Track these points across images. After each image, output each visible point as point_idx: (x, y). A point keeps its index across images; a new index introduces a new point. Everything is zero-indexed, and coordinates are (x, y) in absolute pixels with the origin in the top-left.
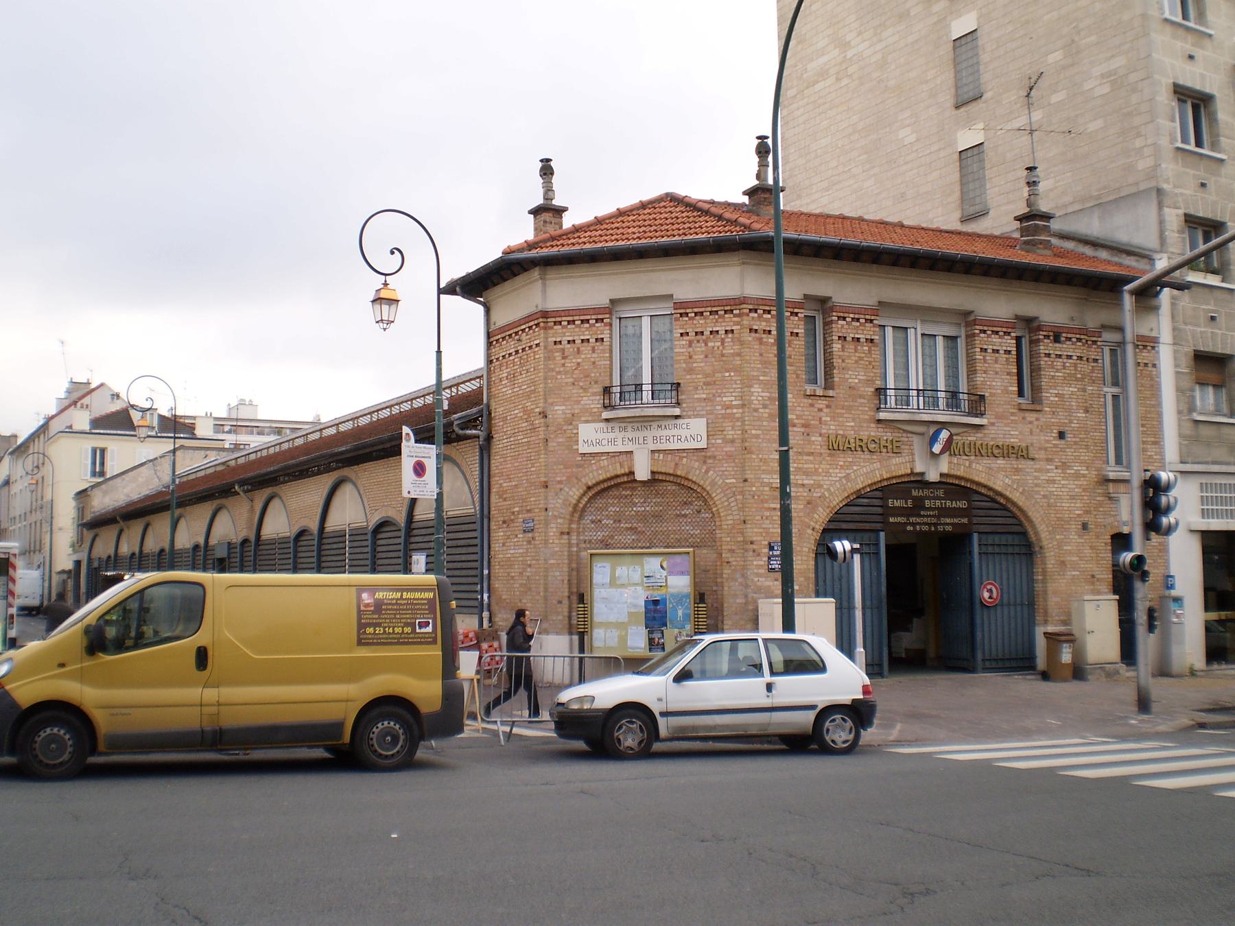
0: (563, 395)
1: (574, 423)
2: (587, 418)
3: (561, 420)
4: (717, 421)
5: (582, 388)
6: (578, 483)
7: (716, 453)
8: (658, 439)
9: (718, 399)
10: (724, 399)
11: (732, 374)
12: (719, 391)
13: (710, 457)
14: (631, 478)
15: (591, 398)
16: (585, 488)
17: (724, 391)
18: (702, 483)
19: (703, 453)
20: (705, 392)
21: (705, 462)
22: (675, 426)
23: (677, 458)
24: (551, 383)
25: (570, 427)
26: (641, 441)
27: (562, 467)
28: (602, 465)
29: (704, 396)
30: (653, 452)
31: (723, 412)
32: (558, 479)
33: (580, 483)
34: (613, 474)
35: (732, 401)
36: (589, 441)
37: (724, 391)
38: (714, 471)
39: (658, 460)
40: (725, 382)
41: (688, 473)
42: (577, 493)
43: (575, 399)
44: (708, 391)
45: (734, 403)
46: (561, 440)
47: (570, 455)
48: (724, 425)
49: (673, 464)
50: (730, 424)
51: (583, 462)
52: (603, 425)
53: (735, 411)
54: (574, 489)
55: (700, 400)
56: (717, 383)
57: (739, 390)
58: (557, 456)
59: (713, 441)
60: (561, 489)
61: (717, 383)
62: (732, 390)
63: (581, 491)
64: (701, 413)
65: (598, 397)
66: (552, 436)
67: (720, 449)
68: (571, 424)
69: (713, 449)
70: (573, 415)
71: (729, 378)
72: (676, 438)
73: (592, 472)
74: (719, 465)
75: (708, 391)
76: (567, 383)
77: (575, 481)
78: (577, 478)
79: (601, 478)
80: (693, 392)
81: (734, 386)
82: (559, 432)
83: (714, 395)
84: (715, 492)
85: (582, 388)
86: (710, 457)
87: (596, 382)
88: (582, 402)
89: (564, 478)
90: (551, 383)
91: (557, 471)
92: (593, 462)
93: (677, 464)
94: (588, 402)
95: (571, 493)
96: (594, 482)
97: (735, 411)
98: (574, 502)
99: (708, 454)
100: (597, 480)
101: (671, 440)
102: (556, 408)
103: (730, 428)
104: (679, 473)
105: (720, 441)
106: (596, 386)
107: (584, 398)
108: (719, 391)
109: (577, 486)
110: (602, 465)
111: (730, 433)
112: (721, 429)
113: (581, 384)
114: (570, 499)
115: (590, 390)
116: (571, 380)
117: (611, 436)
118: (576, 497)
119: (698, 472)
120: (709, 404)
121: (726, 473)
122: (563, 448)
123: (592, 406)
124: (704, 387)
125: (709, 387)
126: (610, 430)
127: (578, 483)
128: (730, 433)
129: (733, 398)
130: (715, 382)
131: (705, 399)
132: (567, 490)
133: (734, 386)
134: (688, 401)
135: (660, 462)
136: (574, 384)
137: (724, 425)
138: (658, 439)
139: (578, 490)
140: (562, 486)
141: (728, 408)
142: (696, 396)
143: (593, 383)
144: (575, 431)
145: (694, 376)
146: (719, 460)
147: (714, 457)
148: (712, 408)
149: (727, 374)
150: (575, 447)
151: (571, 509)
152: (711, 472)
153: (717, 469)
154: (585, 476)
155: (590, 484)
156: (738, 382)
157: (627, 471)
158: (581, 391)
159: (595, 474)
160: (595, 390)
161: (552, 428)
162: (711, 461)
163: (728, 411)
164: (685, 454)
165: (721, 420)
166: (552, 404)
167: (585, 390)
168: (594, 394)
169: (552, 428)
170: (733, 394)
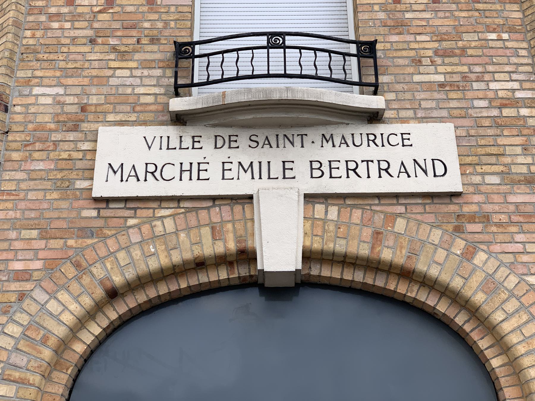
0: (62, 64)
1: (85, 126)
2: (119, 117)
3: (47, 118)
4: (481, 131)
5: (114, 49)
6: (78, 279)
7: (488, 208)
8: (326, 169)
9: (475, 85)
10: (493, 86)
11: (505, 36)
12: (478, 69)
13: (472, 218)
14: (242, 271)
15: (138, 73)
16: (100, 293)
17: (491, 68)
18: (457, 283)
19: (452, 208)
20: (441, 69)
21: (458, 230)
22: (372, 140)
23: (379, 219)
24: (33, 37)
25: (71, 136)
26: (277, 170)
27: (34, 233)
28: (159, 229)
29: (440, 78)
30: (307, 197)
31: (495, 112)
32: (18, 266)
33: (86, 280)
34: (188, 256)
35: (513, 90)
36: (127, 170)
37: (491, 68)
38: (490, 253)
39: (325, 221)
40: (492, 52)
41: (413, 254)
42: (74, 307)
43: (94, 73)
44: (449, 69)
45: (519, 95)
46: (41, 166)
47: (64, 205)
48: (501, 141)
49: (367, 233)
50: (519, 140)
51: (100, 223)
52: (172, 131)
53: (524, 112)
54: (63, 296)
55: (429, 86)
56: (470, 52)
57: (529, 69)
58: (22, 205)
59: (477, 179)
60: (22, 296)
61: (470, 52)
62: (508, 68)
63: (87, 301)
64: (435, 114)
65: (158, 72)
66: (15, 156)
67: (496, 198)
68: (75, 128)
69: (477, 198)
70: (83, 109)
71: (499, 44)
72: (374, 167)
73: (127, 249)
74: (500, 238)
75: (449, 69)
76: (74, 38)
77: (70, 271)
78: (77, 265)
79: (153, 265)
80: (411, 70)
81: (514, 60)
82: (38, 146)
83: (465, 78)
84: (500, 307)
85: (114, 49)
86: (472, 218)
87: (154, 40)
88: (113, 81)
89: (38, 264)
90: (33, 37)
91: (18, 245)
92: (131, 222)
93: (378, 233)
94: (129, 81)
95: (53, 306)
96: (130, 274)
97: (524, 112)
98: (61, 331)
99: (466, 209)
100: (142, 269)
101: (362, 169)
102: (37, 90)
103: (519, 150)
104: (386, 255)
105: (495, 180)
106: (155, 48)
107: (118, 73)
108: (478, 69)
109: (75, 287)
110: (159, 229)
111: (521, 160)
112: (494, 150)
113: (113, 41)
114: (50, 324)
115: (137, 56)
116: (89, 33)
117: (195, 156)
118: (68, 318)
119: (441, 255)
120: (453, 95)
121: (525, 258)
122: (48, 185)
123: (142, 90)
124: (439, 60)
125: (447, 60)
126: (187, 142)
127: (78, 279)
128: (521, 160)
129: (516, 85)
130: (463, 49)
131: (442, 85)
132: (41, 296)
133: (514, 60)
134: (399, 87)
135: (332, 227)
136: (92, 41)
137: (501, 141)
138: (326, 169)
139: (76, 299)
140: (28, 286)
141: (505, 106)
142: (417, 78)
143: (144, 41)
144: (86, 146)
145: (411, 38)
146: (499, 224)
147: (486, 219)
148: (463, 104)
149: (493, 36)
150: (85, 184)
151: (47, 354)
152: (480, 257)
153: (497, 248)
154: (102, 260)
155: (118, 280)
156: (524, 53)
157: (232, 246)
158: (112, 56)
159: (137, 253)
160: (148, 56)
161: (18, 137)
162: (477, 227)
163: (506, 112)
164: (401, 209)
165: (490, 132)
166: (27, 82)
167: (123, 55)
168: (146, 65)
169: (18, 137)
170: (514, 76)
